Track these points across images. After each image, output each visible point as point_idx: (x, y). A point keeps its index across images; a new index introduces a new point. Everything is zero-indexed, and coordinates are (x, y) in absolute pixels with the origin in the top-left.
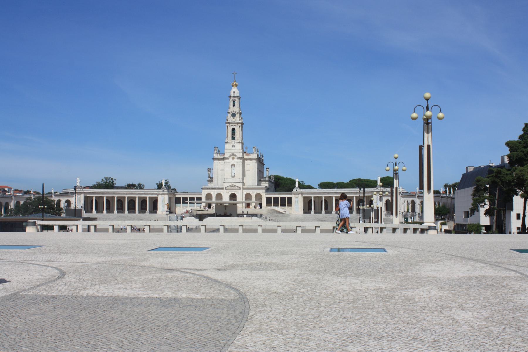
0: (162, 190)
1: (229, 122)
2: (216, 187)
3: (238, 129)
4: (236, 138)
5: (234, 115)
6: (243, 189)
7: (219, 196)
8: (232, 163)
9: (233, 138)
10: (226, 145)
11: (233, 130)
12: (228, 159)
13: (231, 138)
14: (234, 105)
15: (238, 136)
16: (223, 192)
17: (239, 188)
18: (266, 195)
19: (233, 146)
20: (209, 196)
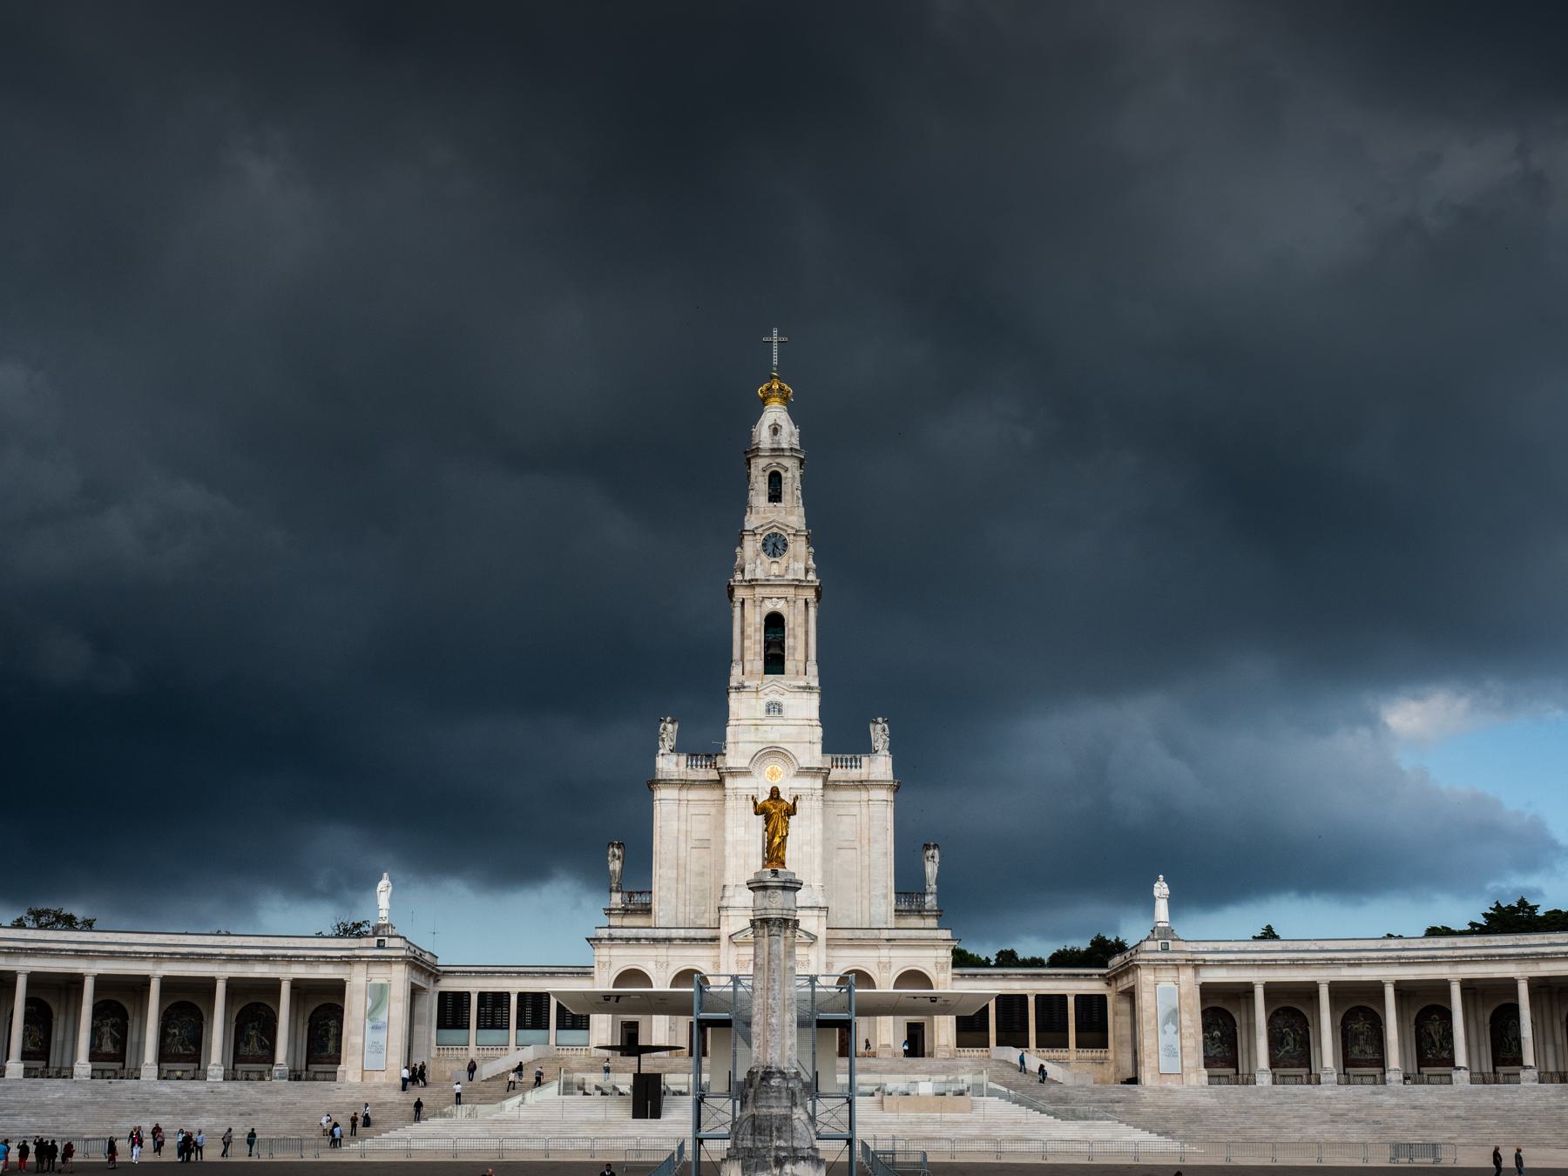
0: (374, 942)
1: (747, 577)
2: (674, 933)
3: (801, 619)
4: (789, 665)
5: (775, 545)
9: (774, 662)
10: (737, 703)
11: (774, 622)
14: (775, 496)
15: (800, 655)
18: (953, 979)
19: (774, 708)
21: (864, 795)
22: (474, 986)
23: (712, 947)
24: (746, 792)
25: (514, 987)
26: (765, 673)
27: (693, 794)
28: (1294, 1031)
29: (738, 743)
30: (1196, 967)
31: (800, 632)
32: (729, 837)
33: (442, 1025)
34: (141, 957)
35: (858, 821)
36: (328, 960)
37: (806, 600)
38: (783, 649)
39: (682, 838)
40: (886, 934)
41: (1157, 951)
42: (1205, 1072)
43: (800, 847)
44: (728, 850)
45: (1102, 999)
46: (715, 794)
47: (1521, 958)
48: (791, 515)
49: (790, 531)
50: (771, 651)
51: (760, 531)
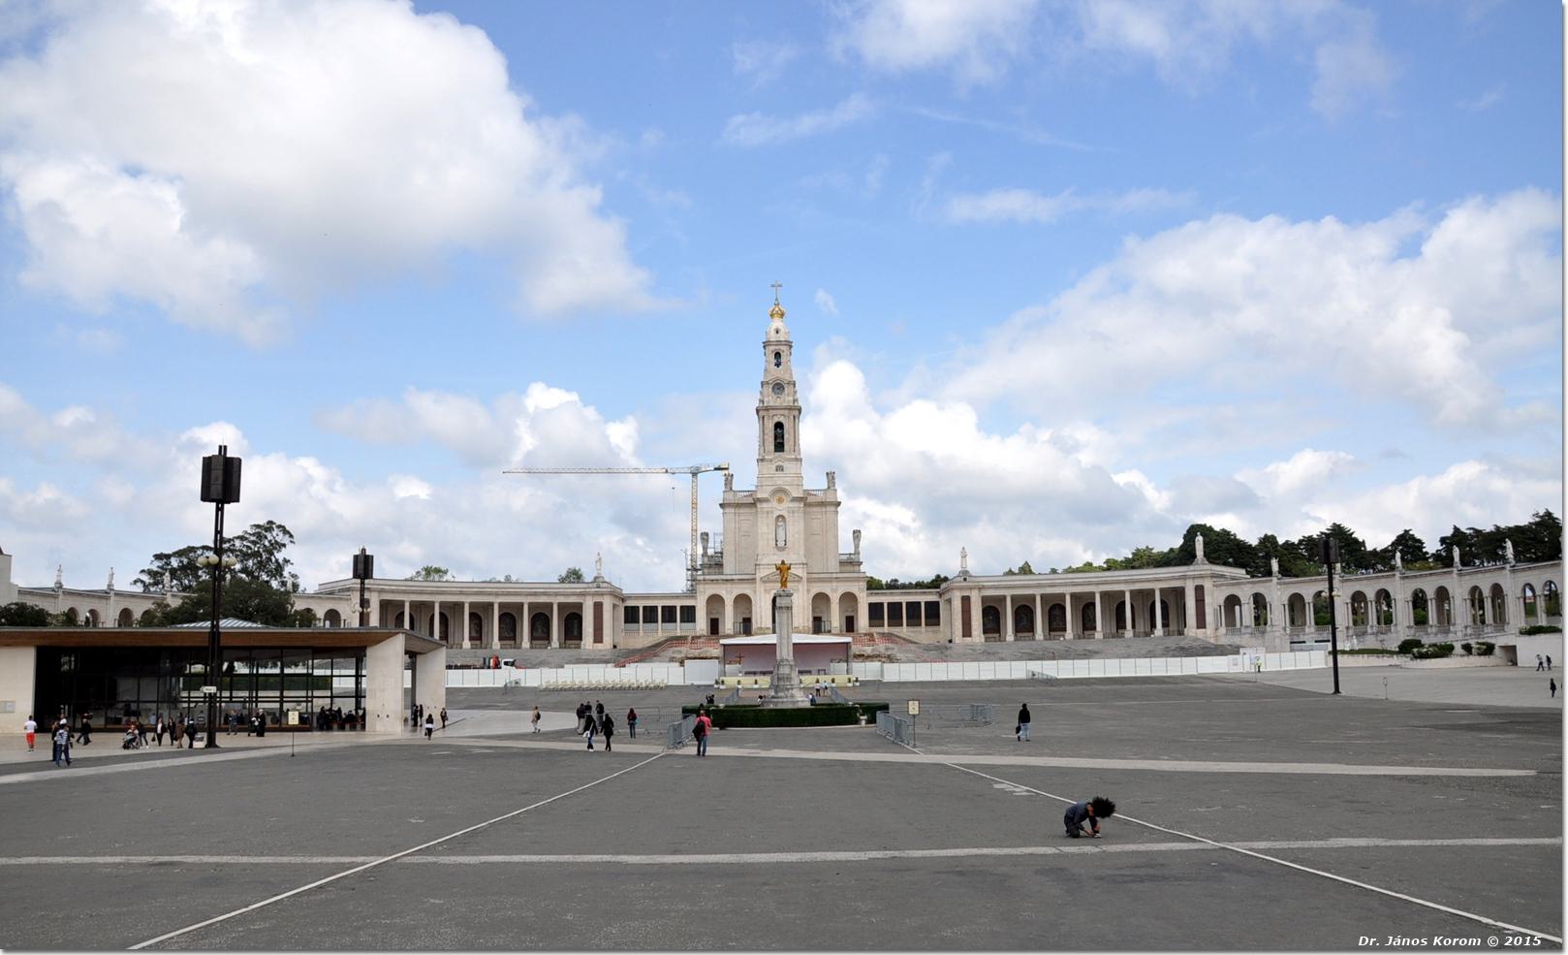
2: (734, 577)
3: (792, 424)
4: (786, 447)
6: (809, 581)
7: (743, 600)
9: (779, 446)
11: (779, 426)
12: (766, 500)
13: (772, 447)
16: (755, 592)
19: (780, 468)
20: (715, 600)
21: (824, 509)
22: (641, 604)
23: (752, 583)
24: (765, 510)
25: (660, 604)
26: (776, 451)
27: (742, 511)
28: (1026, 615)
29: (762, 486)
30: (980, 589)
32: (760, 532)
33: (627, 621)
34: (490, 594)
36: (574, 594)
39: (737, 531)
40: (835, 575)
41: (960, 582)
42: (983, 636)
43: (793, 536)
44: (759, 537)
45: (937, 603)
46: (754, 510)
47: (1126, 582)
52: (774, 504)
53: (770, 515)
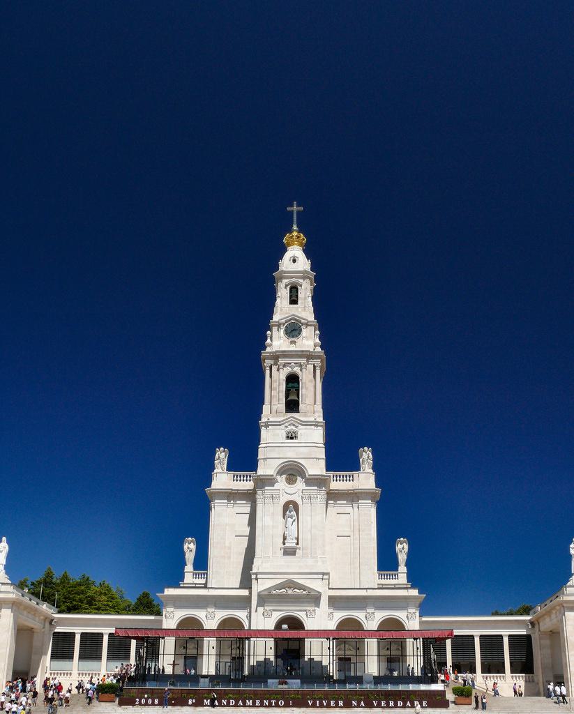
3: (311, 376)
4: (301, 406)
5: (293, 330)
8: (284, 499)
9: (292, 406)
11: (293, 380)
13: (282, 406)
14: (294, 301)
16: (249, 617)
17: (315, 599)
19: (291, 437)
31: (310, 386)
35: (352, 517)
37: (314, 364)
38: (299, 398)
48: (305, 310)
49: (303, 321)
50: (291, 398)
51: (284, 321)
52: (281, 483)
53: (275, 500)
